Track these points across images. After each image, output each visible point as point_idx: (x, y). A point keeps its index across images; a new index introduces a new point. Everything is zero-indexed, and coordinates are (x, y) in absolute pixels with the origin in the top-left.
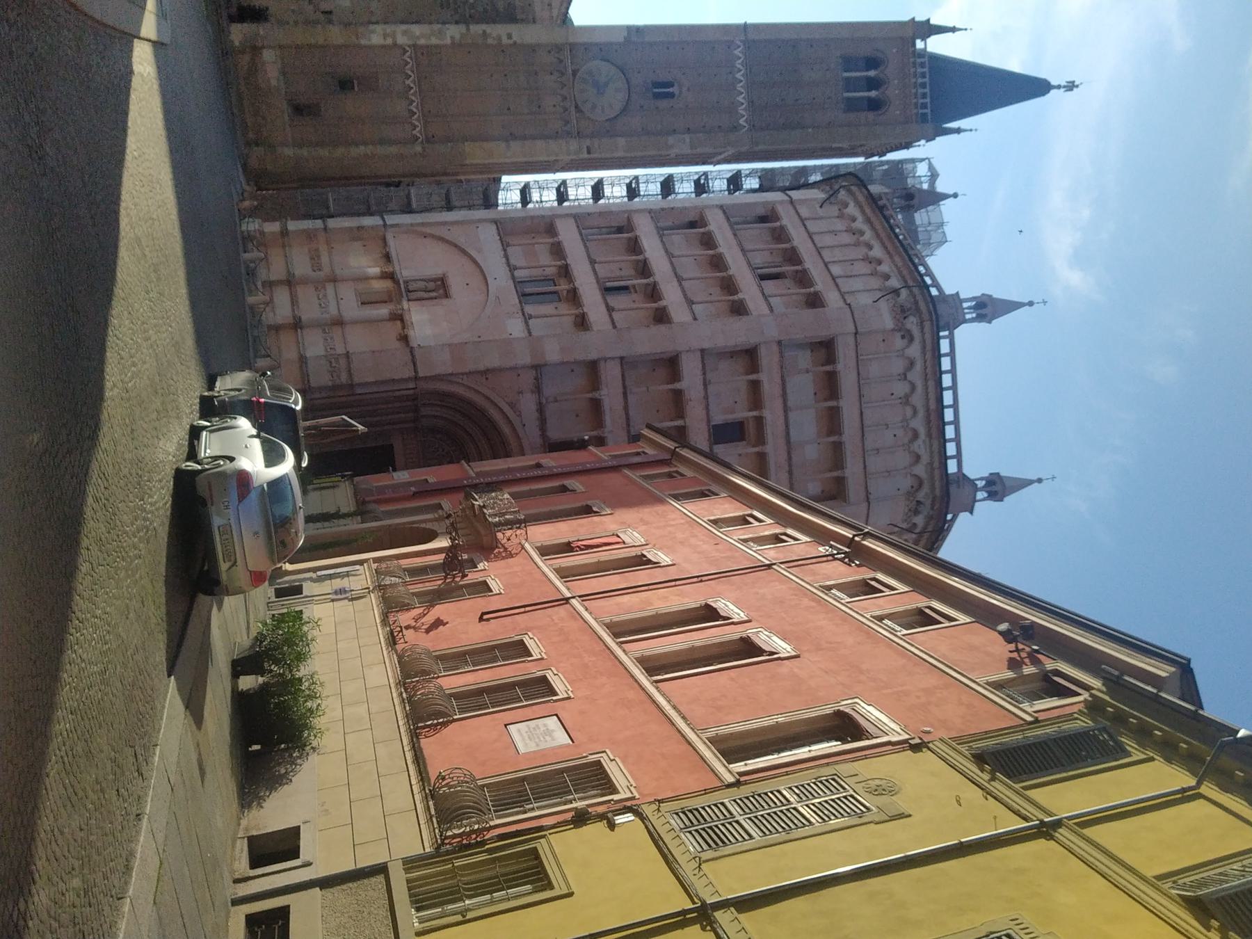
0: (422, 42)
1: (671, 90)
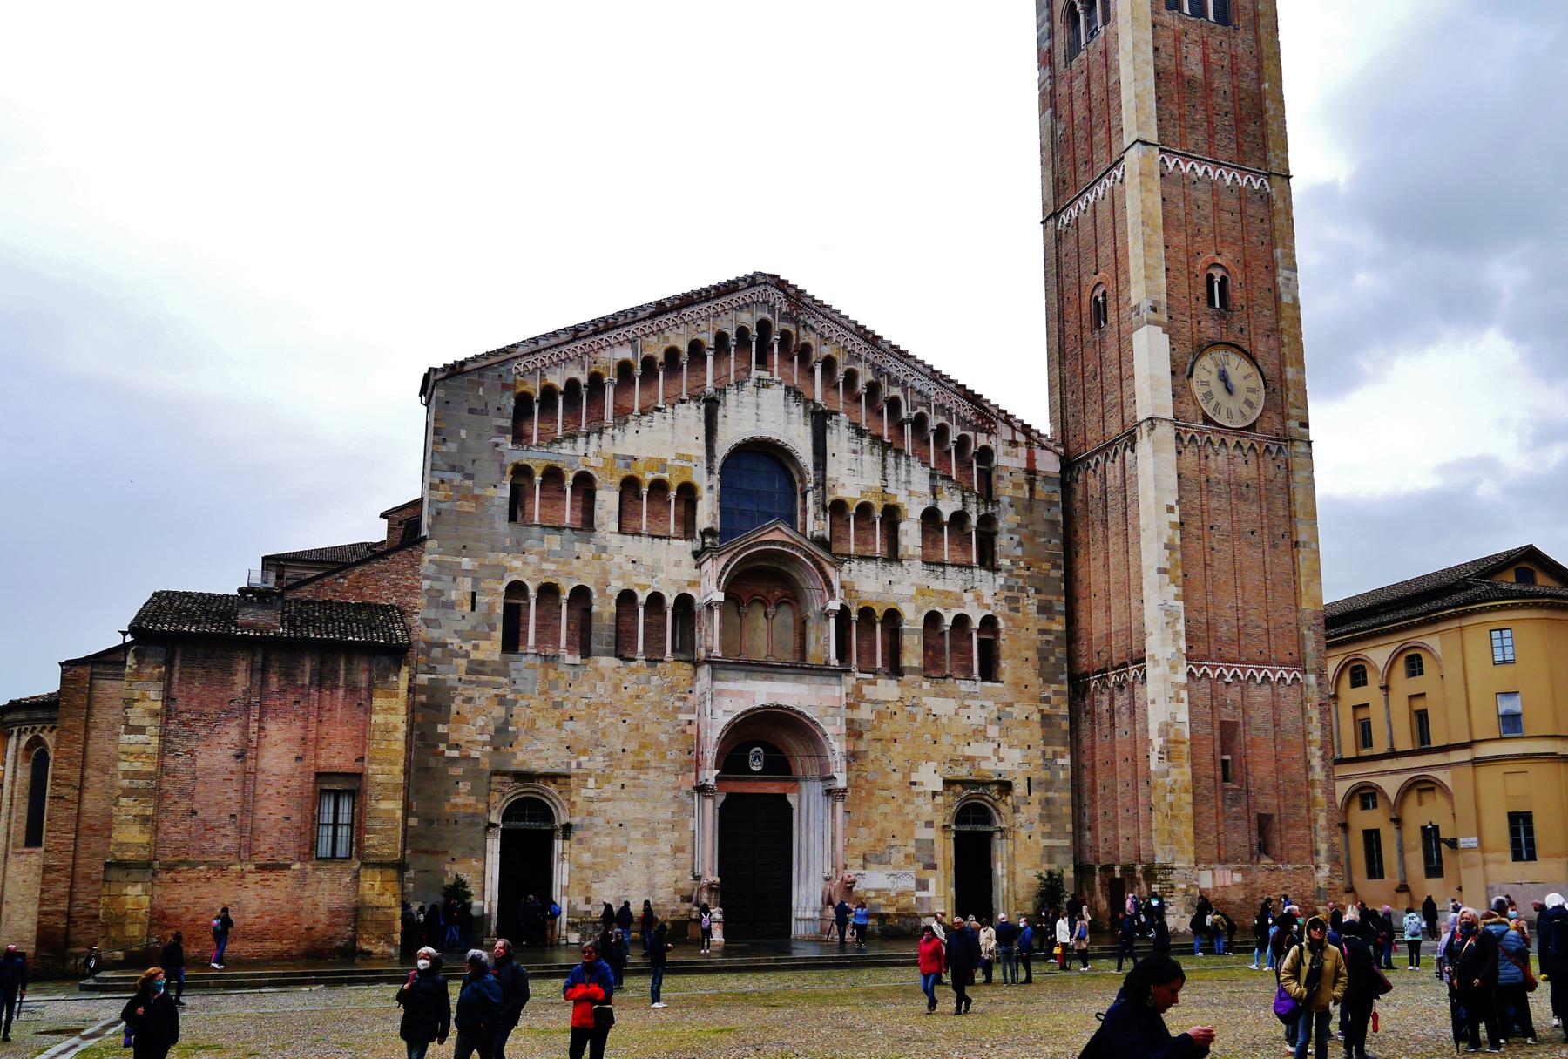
0: (1183, 644)
1: (1217, 279)
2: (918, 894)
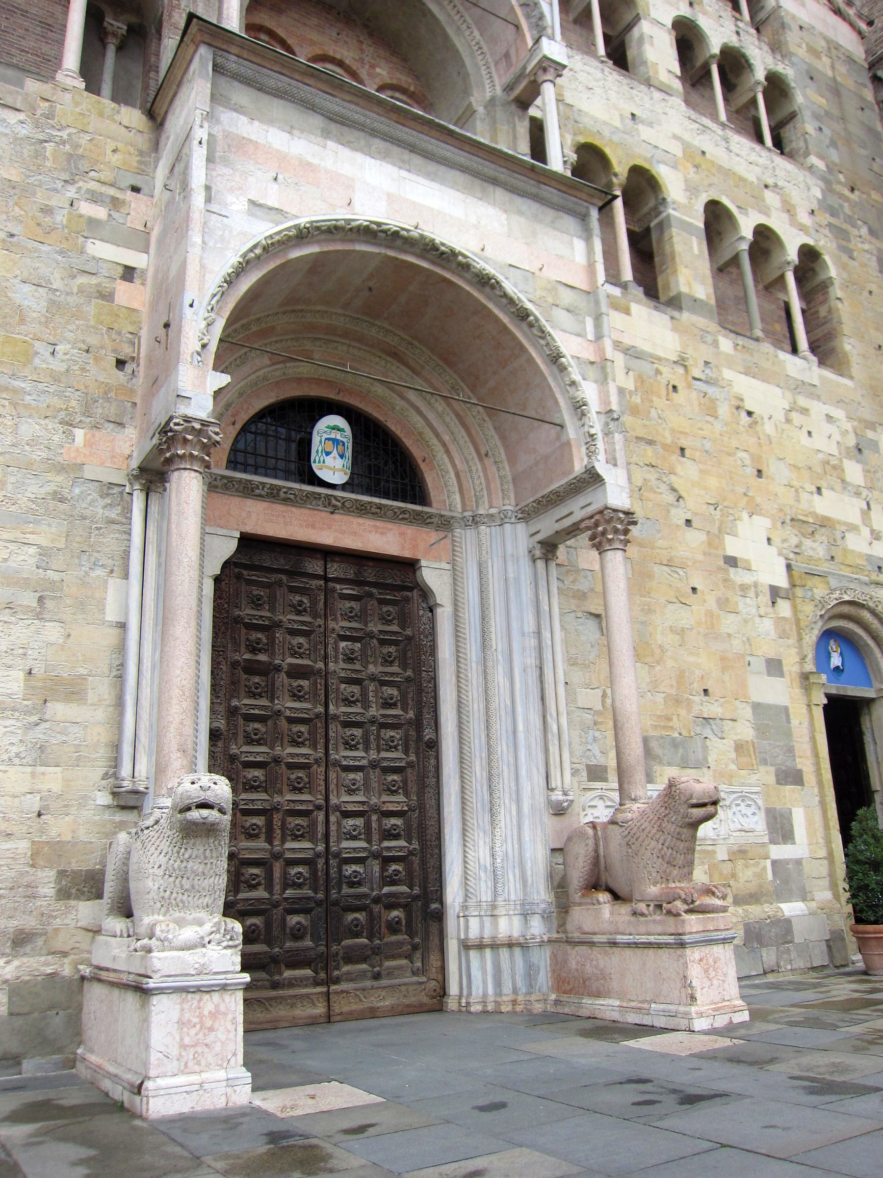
2: (779, 852)
